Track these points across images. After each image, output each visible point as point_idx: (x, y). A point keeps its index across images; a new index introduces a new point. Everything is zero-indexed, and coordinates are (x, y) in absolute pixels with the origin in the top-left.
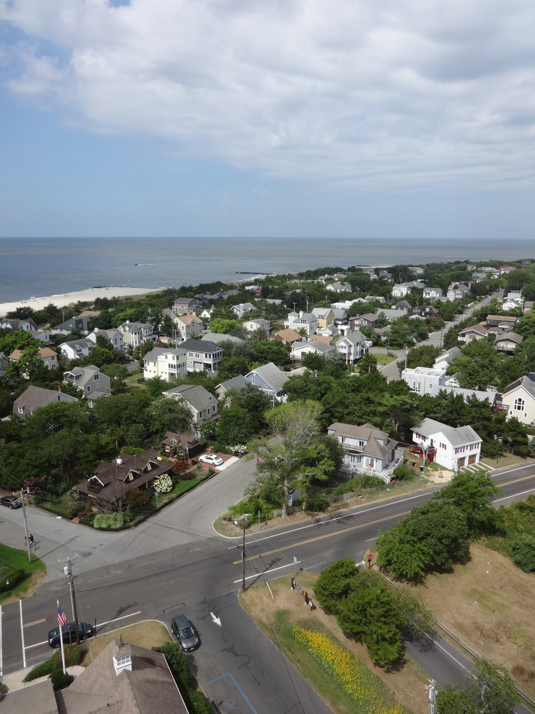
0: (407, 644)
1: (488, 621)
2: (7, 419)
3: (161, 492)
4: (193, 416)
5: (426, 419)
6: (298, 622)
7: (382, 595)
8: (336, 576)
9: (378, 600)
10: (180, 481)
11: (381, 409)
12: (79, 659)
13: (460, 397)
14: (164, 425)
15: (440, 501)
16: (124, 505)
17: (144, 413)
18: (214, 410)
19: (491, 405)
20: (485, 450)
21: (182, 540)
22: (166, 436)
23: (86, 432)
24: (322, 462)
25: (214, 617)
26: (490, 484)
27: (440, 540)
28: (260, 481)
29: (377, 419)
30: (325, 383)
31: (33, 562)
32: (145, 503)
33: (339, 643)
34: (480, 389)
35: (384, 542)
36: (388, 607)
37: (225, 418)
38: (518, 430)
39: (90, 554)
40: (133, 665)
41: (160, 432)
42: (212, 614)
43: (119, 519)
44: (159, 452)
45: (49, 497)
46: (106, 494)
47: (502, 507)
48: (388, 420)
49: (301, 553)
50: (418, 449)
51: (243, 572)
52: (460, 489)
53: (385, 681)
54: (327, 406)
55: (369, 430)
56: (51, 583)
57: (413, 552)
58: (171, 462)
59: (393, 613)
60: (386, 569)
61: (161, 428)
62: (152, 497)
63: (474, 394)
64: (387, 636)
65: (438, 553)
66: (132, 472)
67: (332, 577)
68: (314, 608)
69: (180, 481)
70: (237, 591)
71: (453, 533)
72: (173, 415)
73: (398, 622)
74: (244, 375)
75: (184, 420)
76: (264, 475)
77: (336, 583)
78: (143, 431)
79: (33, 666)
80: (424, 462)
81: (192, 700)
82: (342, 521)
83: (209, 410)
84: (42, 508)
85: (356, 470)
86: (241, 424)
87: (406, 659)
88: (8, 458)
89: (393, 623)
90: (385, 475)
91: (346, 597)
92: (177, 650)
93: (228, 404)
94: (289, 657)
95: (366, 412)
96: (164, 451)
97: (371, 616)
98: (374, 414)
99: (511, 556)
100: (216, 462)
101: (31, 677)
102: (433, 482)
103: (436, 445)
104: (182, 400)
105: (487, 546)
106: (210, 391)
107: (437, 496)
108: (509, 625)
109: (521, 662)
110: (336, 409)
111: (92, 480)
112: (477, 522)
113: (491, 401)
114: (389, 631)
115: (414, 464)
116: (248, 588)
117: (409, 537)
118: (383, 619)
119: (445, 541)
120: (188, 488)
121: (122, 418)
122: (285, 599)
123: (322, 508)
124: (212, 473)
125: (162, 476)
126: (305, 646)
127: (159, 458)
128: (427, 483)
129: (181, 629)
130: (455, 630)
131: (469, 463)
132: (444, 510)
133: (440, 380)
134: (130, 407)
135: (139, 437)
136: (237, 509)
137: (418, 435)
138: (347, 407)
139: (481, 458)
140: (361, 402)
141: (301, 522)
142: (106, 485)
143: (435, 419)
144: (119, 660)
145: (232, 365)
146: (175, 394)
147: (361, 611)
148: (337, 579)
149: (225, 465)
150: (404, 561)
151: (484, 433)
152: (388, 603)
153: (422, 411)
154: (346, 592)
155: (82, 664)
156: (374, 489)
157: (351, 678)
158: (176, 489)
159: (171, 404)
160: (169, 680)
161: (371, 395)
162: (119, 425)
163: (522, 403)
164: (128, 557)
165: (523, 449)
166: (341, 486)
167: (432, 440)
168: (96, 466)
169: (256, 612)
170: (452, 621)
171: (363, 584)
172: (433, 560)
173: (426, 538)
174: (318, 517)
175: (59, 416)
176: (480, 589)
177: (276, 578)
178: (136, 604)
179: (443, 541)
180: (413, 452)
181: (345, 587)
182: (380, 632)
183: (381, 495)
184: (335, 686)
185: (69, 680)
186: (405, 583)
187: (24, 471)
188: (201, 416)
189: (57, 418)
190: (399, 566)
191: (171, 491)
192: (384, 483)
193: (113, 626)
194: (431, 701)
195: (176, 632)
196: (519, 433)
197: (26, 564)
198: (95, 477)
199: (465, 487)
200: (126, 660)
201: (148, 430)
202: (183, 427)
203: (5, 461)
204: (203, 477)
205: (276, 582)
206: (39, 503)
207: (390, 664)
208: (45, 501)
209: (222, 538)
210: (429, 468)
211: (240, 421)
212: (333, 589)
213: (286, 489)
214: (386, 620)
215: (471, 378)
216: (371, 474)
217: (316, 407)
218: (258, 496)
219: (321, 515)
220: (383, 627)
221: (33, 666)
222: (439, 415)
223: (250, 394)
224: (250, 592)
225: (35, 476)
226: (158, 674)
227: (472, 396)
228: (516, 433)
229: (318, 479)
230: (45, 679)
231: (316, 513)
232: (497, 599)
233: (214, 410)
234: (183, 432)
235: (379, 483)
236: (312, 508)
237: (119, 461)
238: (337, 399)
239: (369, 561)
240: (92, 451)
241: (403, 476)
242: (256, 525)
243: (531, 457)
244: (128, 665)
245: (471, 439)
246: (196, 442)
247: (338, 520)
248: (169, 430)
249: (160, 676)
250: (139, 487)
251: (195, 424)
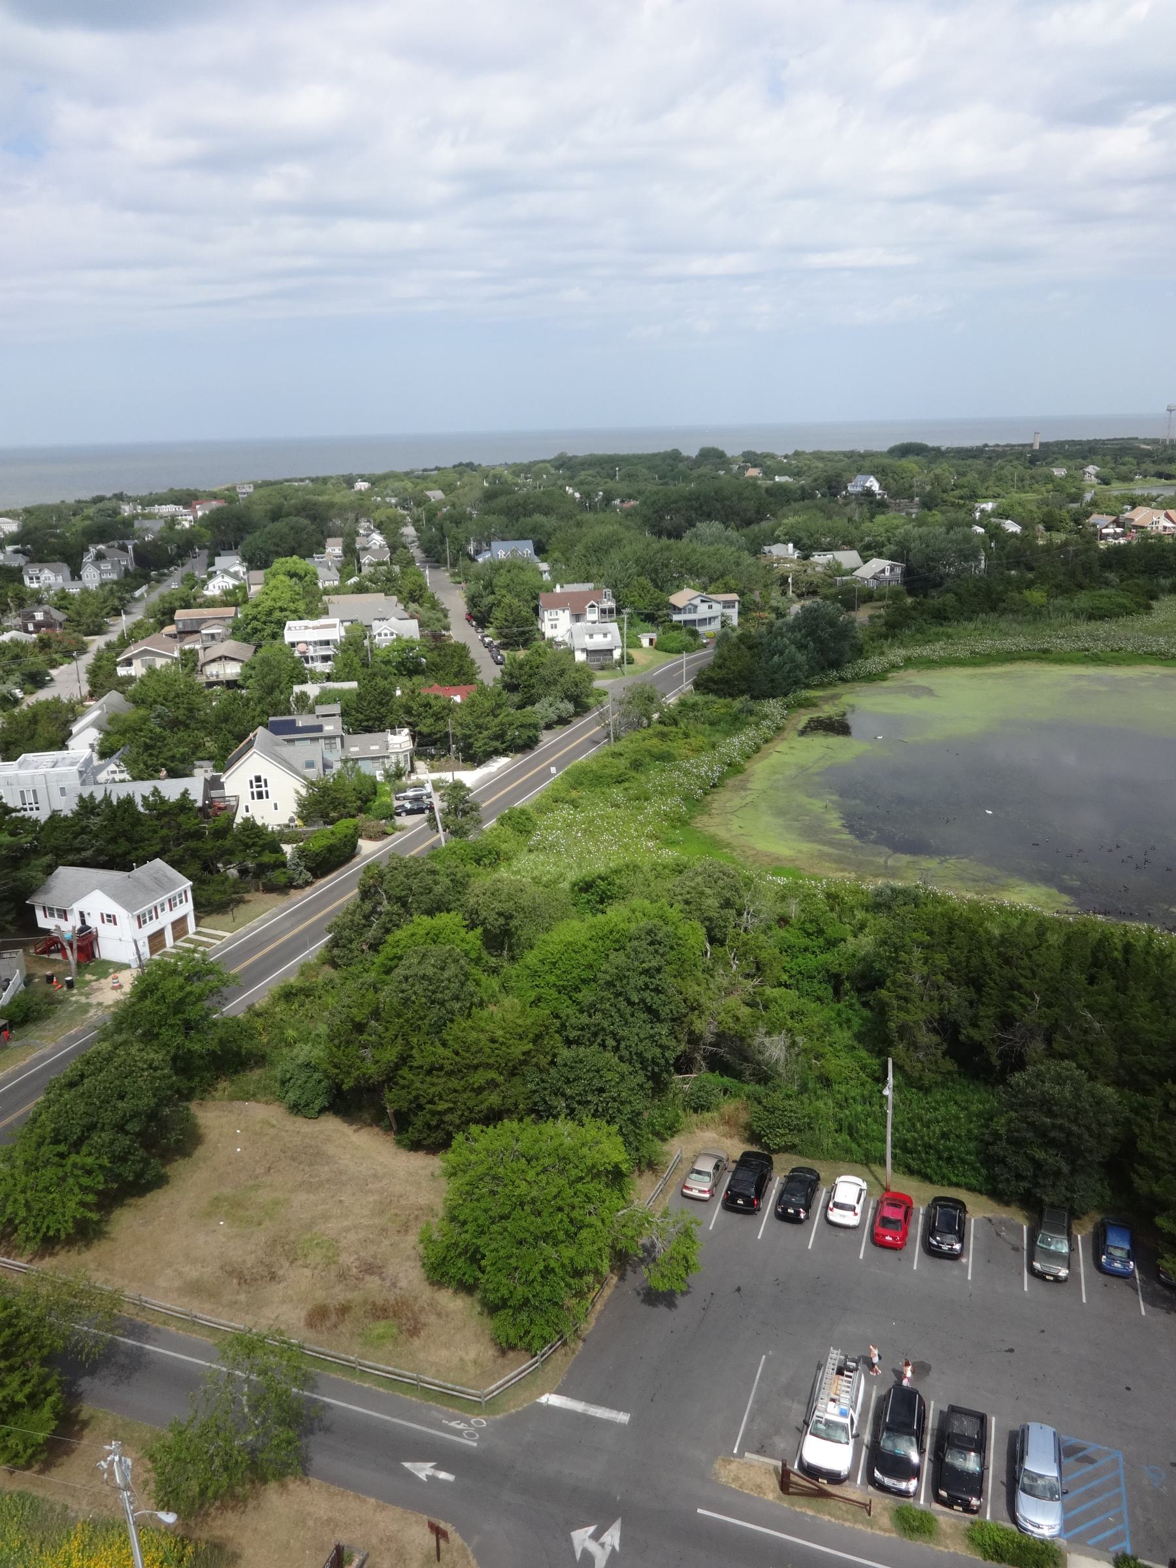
1: (245, 1250)
5: (61, 869)
13: (129, 802)
15: (106, 1046)
19: (199, 804)
20: (203, 900)
26: (210, 972)
27: (121, 1128)
34: (174, 774)
38: (261, 842)
47: (250, 1008)
50: (51, 943)
52: (148, 1002)
53: (40, 1493)
57: (63, 1179)
63: (156, 789)
64: (20, 1398)
65: (123, 1159)
71: (147, 1102)
73: (45, 1351)
80: (73, 967)
89: (32, 1358)
99: (280, 1099)
102: (100, 1004)
103: (93, 922)
105: (233, 1098)
107: (105, 1035)
108: (292, 1237)
109: (320, 1295)
112: (201, 1057)
113: (197, 795)
114: (24, 1383)
115: (50, 979)
117: (47, 1151)
119: (134, 1127)
128: (87, 1012)
130: (186, 1300)
131: (175, 939)
132: (117, 1061)
133: (81, 773)
137: (49, 911)
139: (198, 920)
143: (84, 864)
150: (46, 1207)
151: (195, 867)
153: (46, 854)
163: (263, 783)
165: (278, 876)
167: (82, 914)
170: (177, 1284)
172: (118, 1177)
173: (88, 1137)
176: (227, 1191)
179: (128, 1127)
180: (43, 952)
186: (63, 1253)
190: (35, 1223)
194: (122, 1486)
196: (264, 847)
199: (159, 993)
207: (43, 1451)
210: (88, 977)
215: (151, 755)
222: (88, 854)
227: (153, 794)
228: (258, 849)
232: (263, 1196)
241: (26, 1015)
243: (296, 887)
245: (163, 885)
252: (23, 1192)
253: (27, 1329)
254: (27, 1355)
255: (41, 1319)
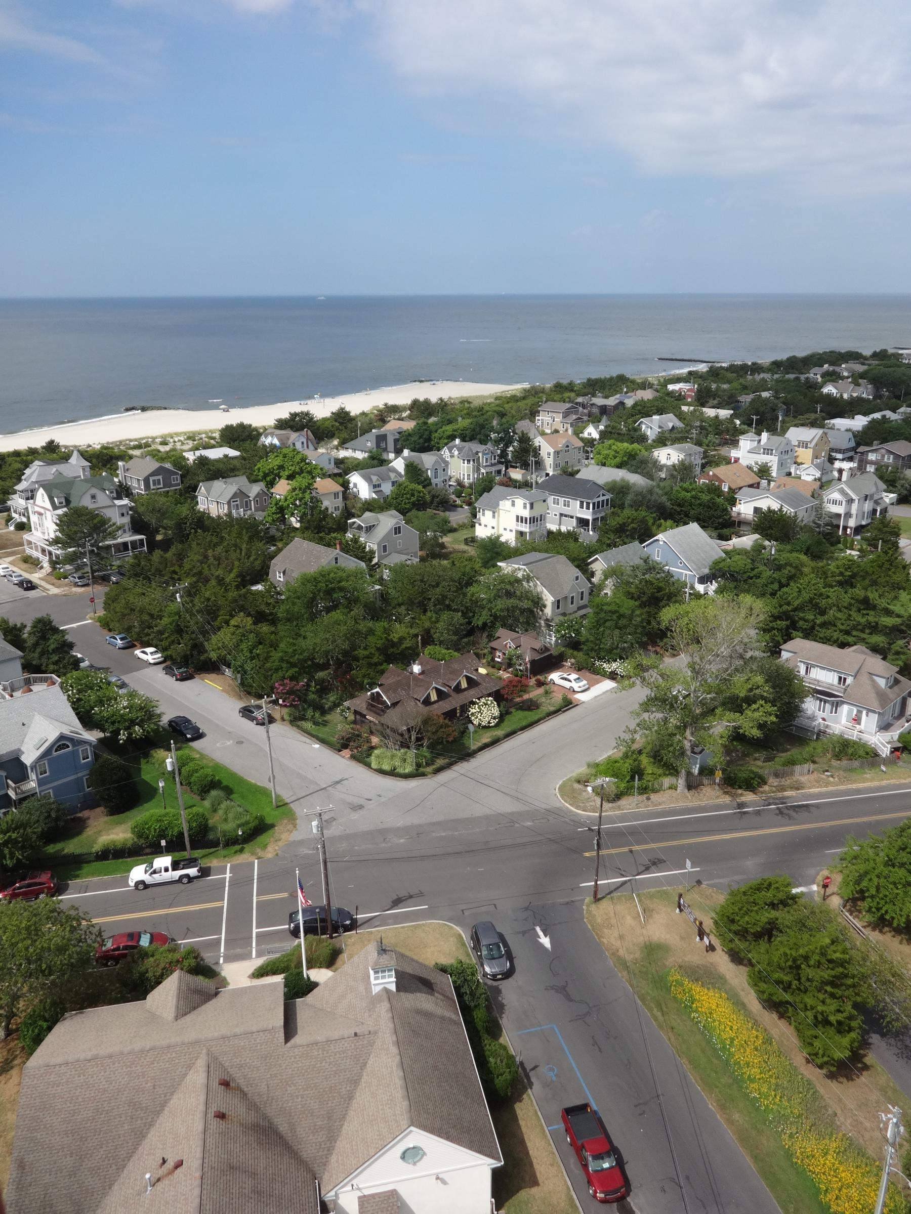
0: (875, 1038)
2: (259, 587)
3: (480, 724)
4: (545, 606)
6: (680, 967)
7: (833, 948)
8: (756, 904)
9: (823, 954)
10: (513, 710)
11: (888, 621)
12: (331, 960)
14: (496, 617)
16: (418, 739)
17: (465, 595)
18: (582, 599)
21: (506, 806)
22: (497, 635)
23: (372, 619)
24: (754, 706)
25: (541, 933)
28: (642, 725)
29: (879, 639)
30: (791, 565)
31: (278, 807)
32: (450, 739)
33: (748, 1014)
35: (856, 858)
36: (841, 970)
37: (598, 613)
39: (361, 807)
40: (397, 983)
41: (488, 629)
42: (538, 929)
43: (409, 760)
44: (484, 661)
45: (310, 713)
46: (393, 718)
48: (901, 642)
49: (700, 855)
51: (594, 872)
53: (822, 1091)
54: (785, 607)
55: (863, 657)
56: (301, 843)
58: (500, 678)
59: (849, 982)
60: (855, 906)
61: (492, 622)
62: (464, 731)
64: (832, 1018)
66: (437, 690)
67: (748, 903)
68: (711, 948)
69: (513, 710)
70: (584, 900)
72: (511, 602)
73: (859, 999)
74: (642, 542)
75: (532, 612)
76: (652, 717)
77: (753, 914)
78: (461, 625)
79: (265, 958)
81: (487, 1053)
82: (786, 811)
83: (573, 598)
84: (298, 727)
85: (827, 726)
86: (625, 627)
87: (868, 1063)
88: (255, 647)
90: (882, 742)
91: (769, 941)
92: (473, 974)
93: (608, 591)
94: (656, 1019)
95: (859, 624)
96: (493, 659)
97: (808, 980)
98: (874, 628)
100: (576, 686)
101: (260, 973)
104: (528, 578)
106: (578, 567)
110: (801, 615)
111: (373, 694)
114: (839, 1011)
116: (603, 898)
118: (829, 988)
120: (524, 724)
121: (430, 599)
122: (665, 927)
123: (752, 783)
124: (568, 704)
125: (483, 700)
126: (687, 1008)
127: (482, 671)
129: (484, 942)
134: (443, 584)
135: (455, 633)
136: (601, 768)
138: (823, 612)
140: (850, 604)
141: (711, 802)
142: (394, 705)
144: (376, 972)
145: (624, 524)
146: (516, 566)
147: (791, 967)
148: (755, 909)
149: (591, 692)
150: (890, 896)
152: (842, 963)
154: (769, 932)
155: (333, 968)
156: (856, 763)
157: (761, 1073)
158: (506, 723)
159: (510, 583)
160: (454, 1017)
161: (873, 595)
162: (425, 611)
164: (417, 821)
166: (794, 752)
168: (382, 672)
169: (610, 938)
171: (802, 925)
174: (743, 799)
175: (333, 589)
177: (653, 890)
178: (421, 894)
181: (769, 923)
182: (820, 1008)
183: (868, 776)
184: (731, 1081)
185: (312, 986)
186: (889, 935)
187: (277, 670)
188: (558, 607)
189: (326, 592)
190: (878, 903)
191: (497, 725)
192: (876, 755)
193: (384, 921)
194: (891, 1141)
195: (477, 947)
197: (268, 809)
198: (378, 689)
200: (387, 974)
201: (470, 623)
202: (528, 623)
203: (251, 653)
204: (552, 709)
205: (651, 896)
206: (296, 720)
207: (833, 1065)
208: (303, 718)
209: (571, 811)
211: (623, 622)
212: (748, 923)
213: (687, 745)
214: (835, 991)
216: (853, 735)
217: (755, 607)
218: (640, 752)
219: (748, 797)
220: (828, 1001)
221: (265, 958)
223: (647, 576)
224: (605, 904)
225: (292, 678)
226: (436, 1004)
229: (744, 735)
230: (279, 979)
231: (740, 791)
233: (582, 599)
234: (527, 630)
235: (867, 753)
236: (731, 782)
237: (416, 668)
238: (806, 596)
239: (825, 886)
240: (378, 649)
242: (631, 798)
244: (389, 981)
246: (547, 649)
247: (778, 808)
248: (504, 626)
249: (441, 1008)
250: (443, 714)
251: (547, 620)
252: (878, 877)
253: (853, 977)
254: (847, 993)
255: (864, 977)
